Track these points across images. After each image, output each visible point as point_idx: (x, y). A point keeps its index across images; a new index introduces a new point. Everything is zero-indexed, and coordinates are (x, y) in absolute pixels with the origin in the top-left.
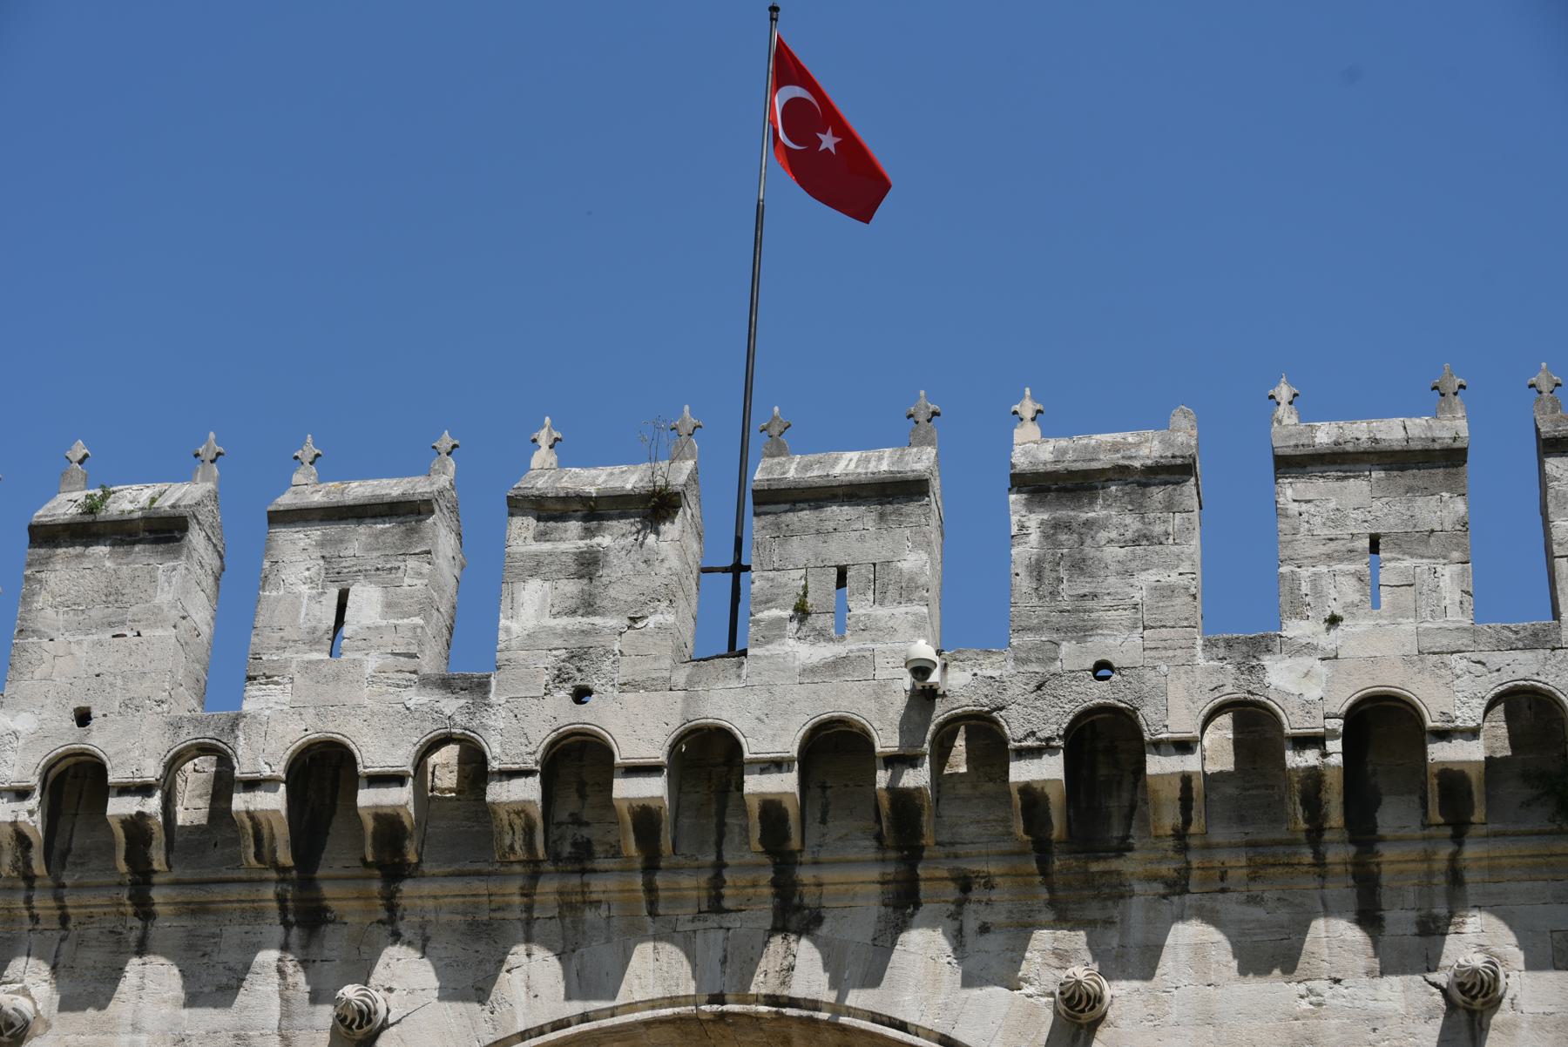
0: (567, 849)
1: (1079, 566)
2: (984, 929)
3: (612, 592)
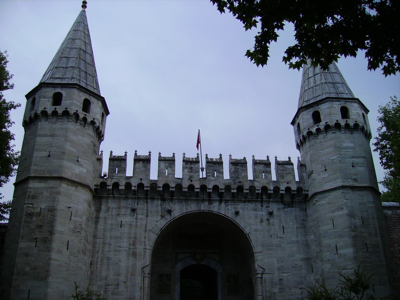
0: (189, 195)
1: (237, 172)
2: (228, 205)
3: (194, 171)
